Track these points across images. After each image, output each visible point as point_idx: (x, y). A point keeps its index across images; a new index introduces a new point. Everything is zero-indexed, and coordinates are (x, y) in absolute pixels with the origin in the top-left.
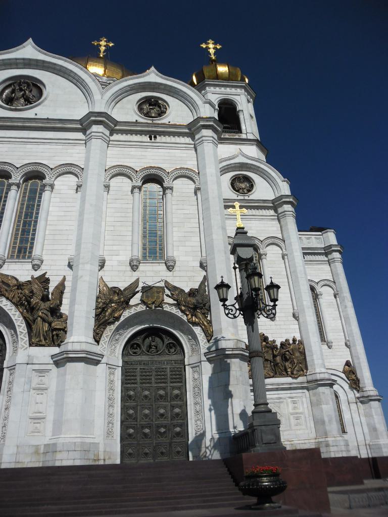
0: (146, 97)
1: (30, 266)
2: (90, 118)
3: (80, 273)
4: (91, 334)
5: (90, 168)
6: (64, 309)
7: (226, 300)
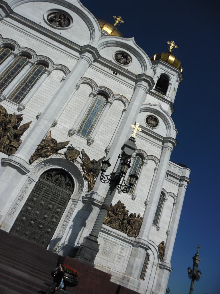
0: (122, 51)
1: (16, 108)
2: (87, 47)
3: (40, 123)
4: (29, 157)
5: (74, 72)
6: (22, 138)
7: (105, 171)
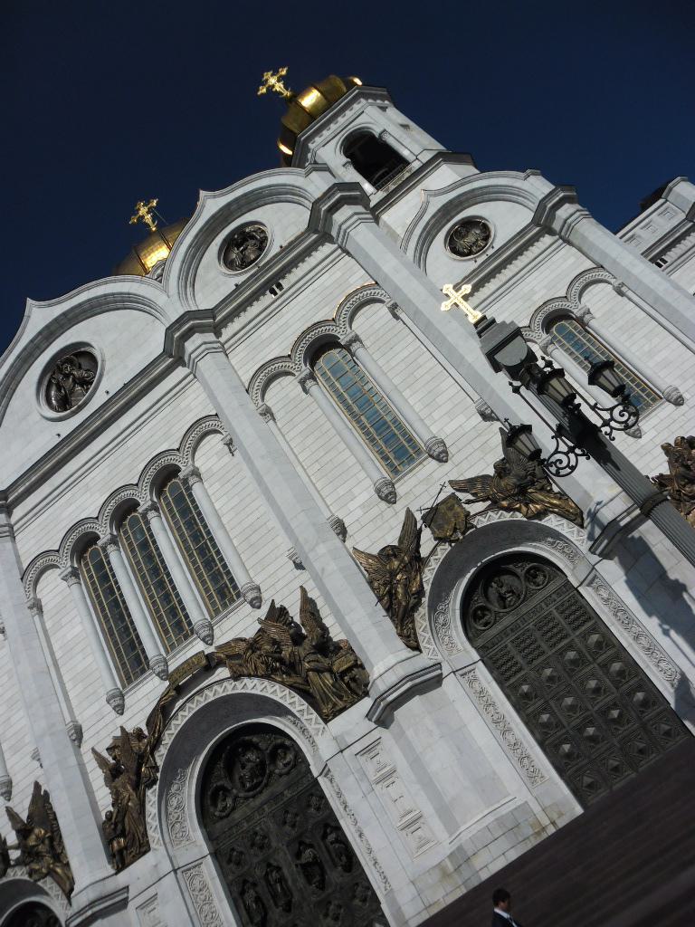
0: (225, 240)
1: (247, 607)
2: (173, 337)
3: (317, 566)
4: (399, 643)
5: (223, 405)
6: (336, 634)
7: (539, 451)
